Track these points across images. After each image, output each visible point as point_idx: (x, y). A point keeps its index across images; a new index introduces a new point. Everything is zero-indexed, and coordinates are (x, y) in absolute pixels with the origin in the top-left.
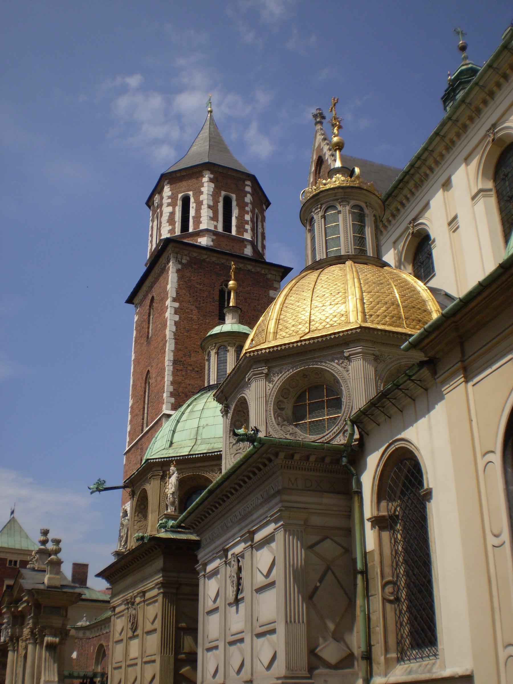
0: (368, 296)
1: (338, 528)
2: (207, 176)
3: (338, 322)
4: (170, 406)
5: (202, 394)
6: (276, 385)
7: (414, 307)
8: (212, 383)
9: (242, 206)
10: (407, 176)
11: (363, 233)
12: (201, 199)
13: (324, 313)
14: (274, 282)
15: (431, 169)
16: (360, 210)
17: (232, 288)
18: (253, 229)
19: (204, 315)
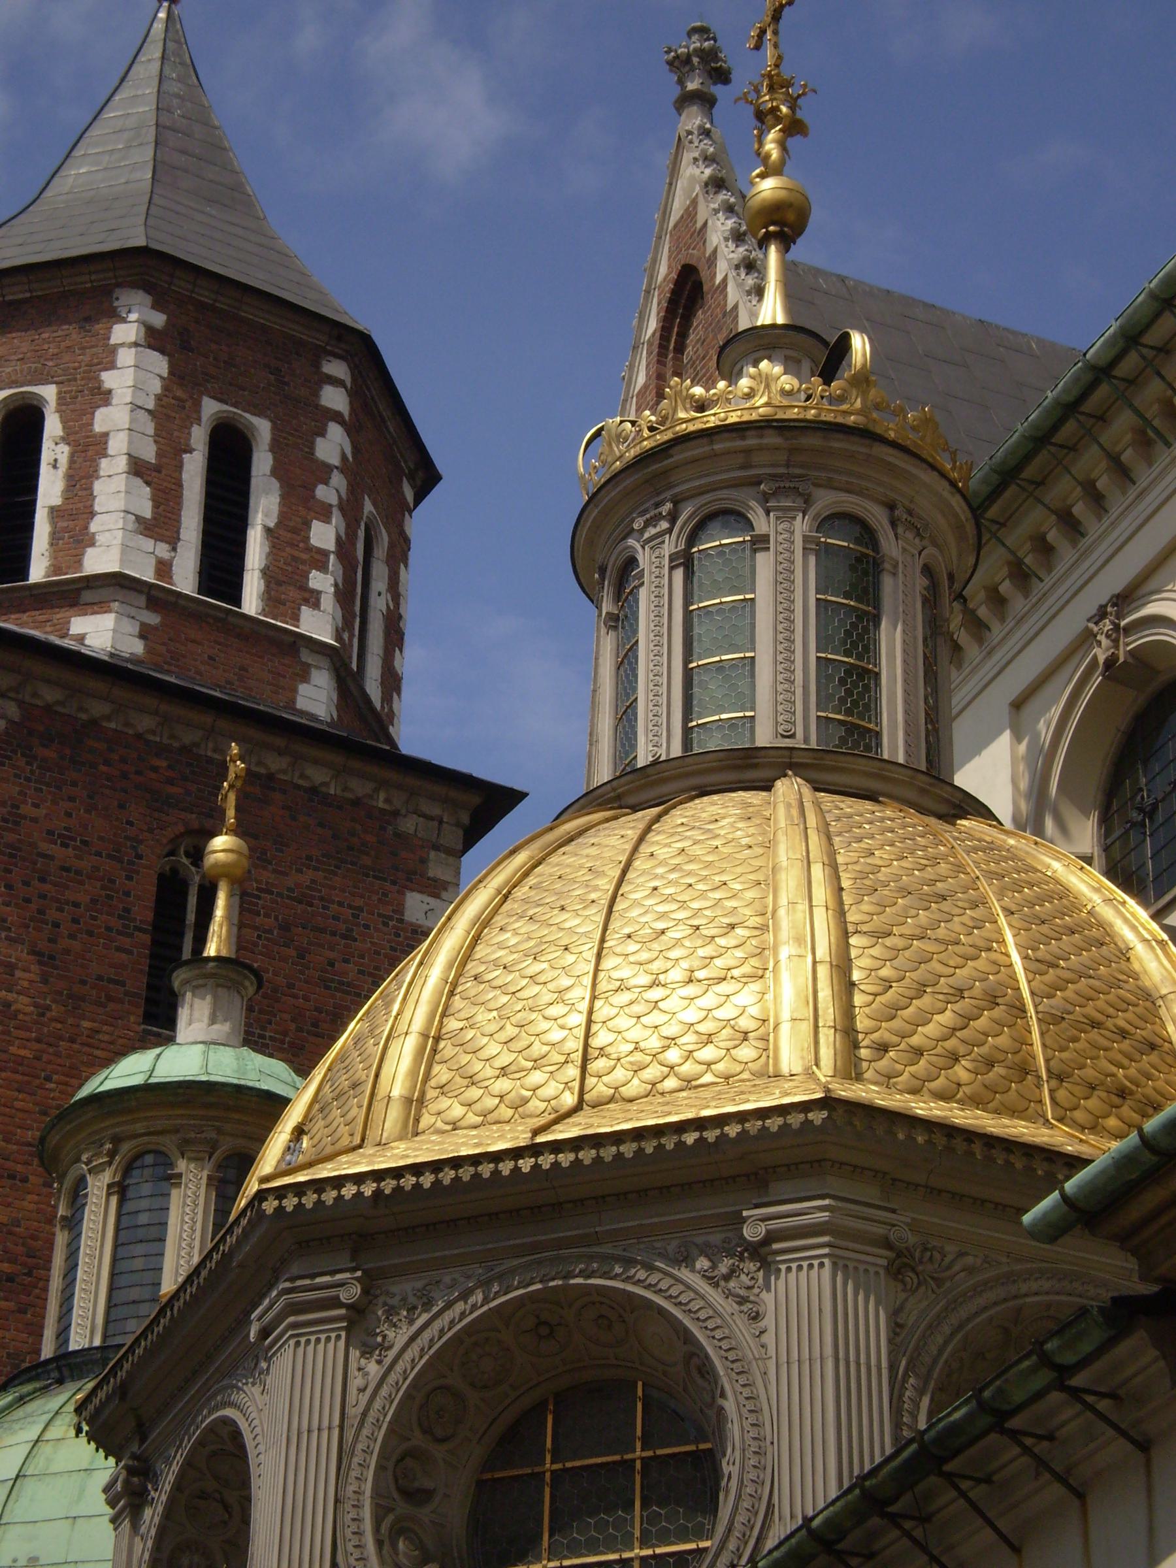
0: (875, 951)
2: (133, 317)
3: (720, 1067)
5: (21, 1401)
6: (399, 1367)
7: (1095, 1024)
8: (77, 1342)
10: (1103, 390)
11: (866, 649)
12: (98, 427)
13: (656, 1018)
14: (432, 854)
16: (858, 541)
17: (224, 871)
18: (344, 596)
19: (70, 996)
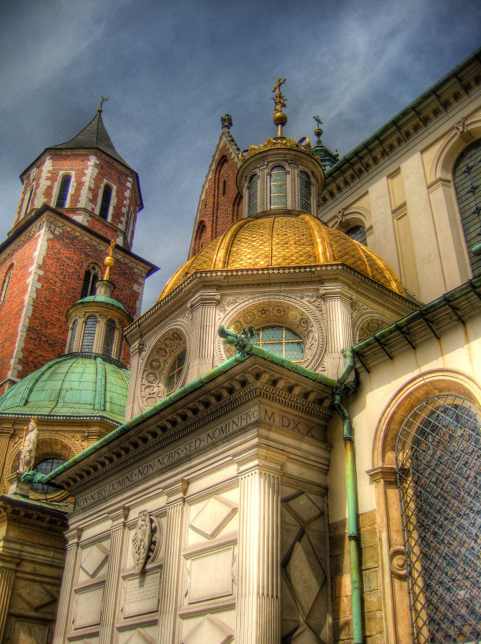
1: (313, 483)
2: (93, 161)
4: (16, 373)
6: (230, 315)
9: (121, 198)
10: (347, 165)
15: (375, 160)
